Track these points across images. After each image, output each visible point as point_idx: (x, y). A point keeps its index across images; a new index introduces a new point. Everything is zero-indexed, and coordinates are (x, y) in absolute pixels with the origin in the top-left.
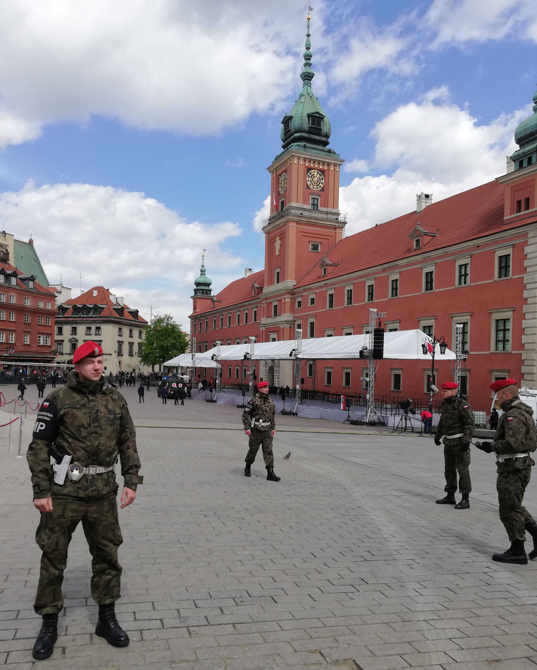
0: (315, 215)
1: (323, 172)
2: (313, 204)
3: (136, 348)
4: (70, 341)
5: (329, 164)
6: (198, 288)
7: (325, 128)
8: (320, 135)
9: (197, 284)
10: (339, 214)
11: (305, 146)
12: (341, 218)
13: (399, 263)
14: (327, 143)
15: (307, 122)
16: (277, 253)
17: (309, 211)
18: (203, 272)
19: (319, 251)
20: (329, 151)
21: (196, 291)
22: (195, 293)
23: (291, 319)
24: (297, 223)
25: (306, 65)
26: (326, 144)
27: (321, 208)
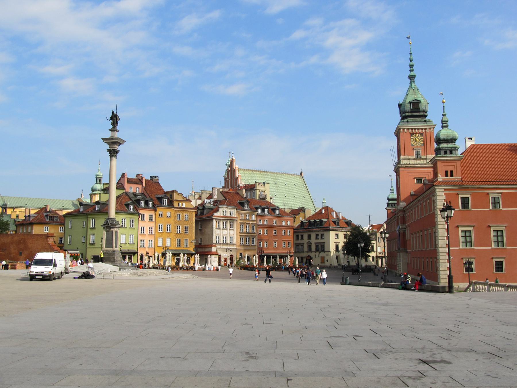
0: (417, 162)
1: (422, 134)
2: (417, 155)
4: (308, 243)
5: (426, 129)
7: (422, 107)
8: (419, 112)
11: (408, 121)
13: (419, 198)
14: (426, 116)
15: (409, 106)
17: (414, 159)
20: (425, 121)
21: (387, 204)
23: (404, 226)
24: (405, 168)
25: (410, 71)
27: (422, 157)
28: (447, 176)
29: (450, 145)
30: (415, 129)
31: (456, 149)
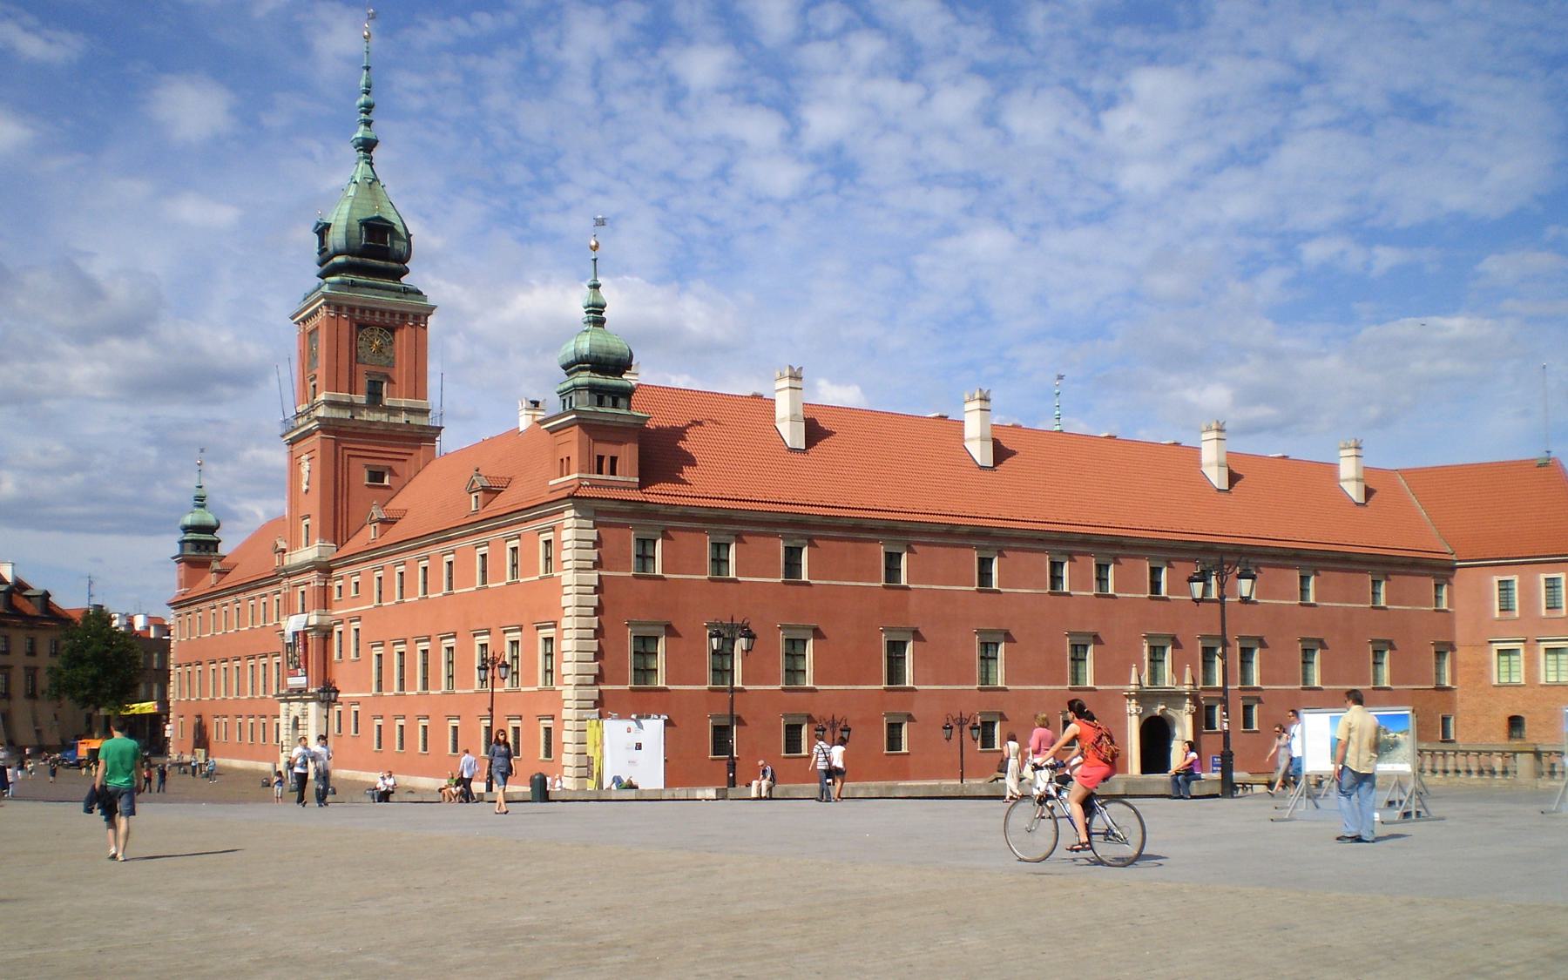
3: (44, 682)
5: (404, 315)
6: (189, 536)
8: (386, 259)
9: (187, 529)
10: (425, 412)
11: (353, 285)
12: (430, 421)
16: (305, 487)
18: (200, 502)
19: (386, 482)
20: (407, 291)
22: (182, 548)
23: (327, 620)
24: (335, 433)
26: (398, 274)
27: (387, 402)
28: (600, 472)
29: (612, 381)
30: (373, 311)
31: (627, 393)
